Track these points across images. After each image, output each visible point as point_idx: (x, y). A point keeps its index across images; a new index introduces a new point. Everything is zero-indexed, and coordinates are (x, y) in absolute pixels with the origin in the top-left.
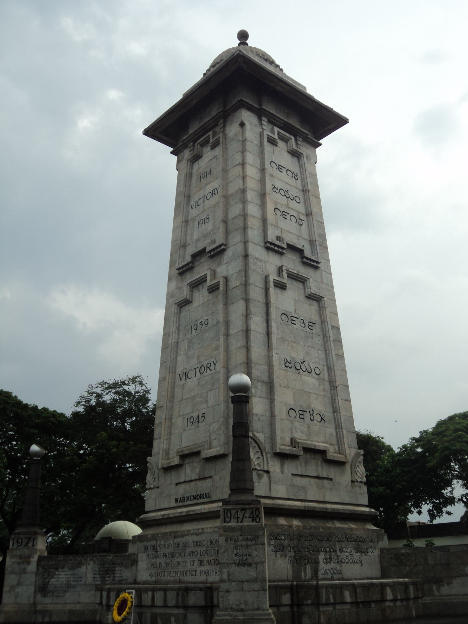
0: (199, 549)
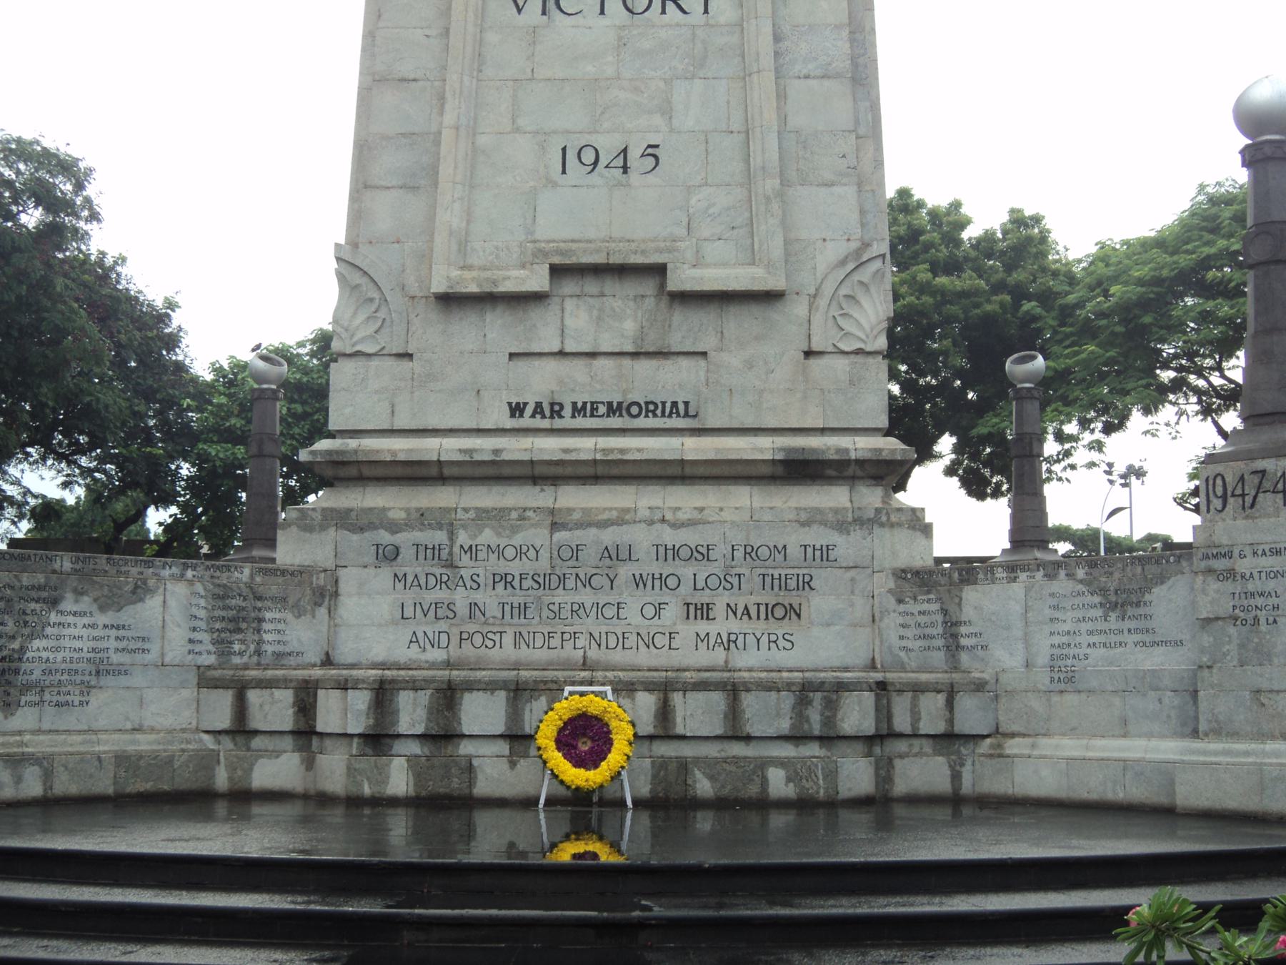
0: (687, 571)
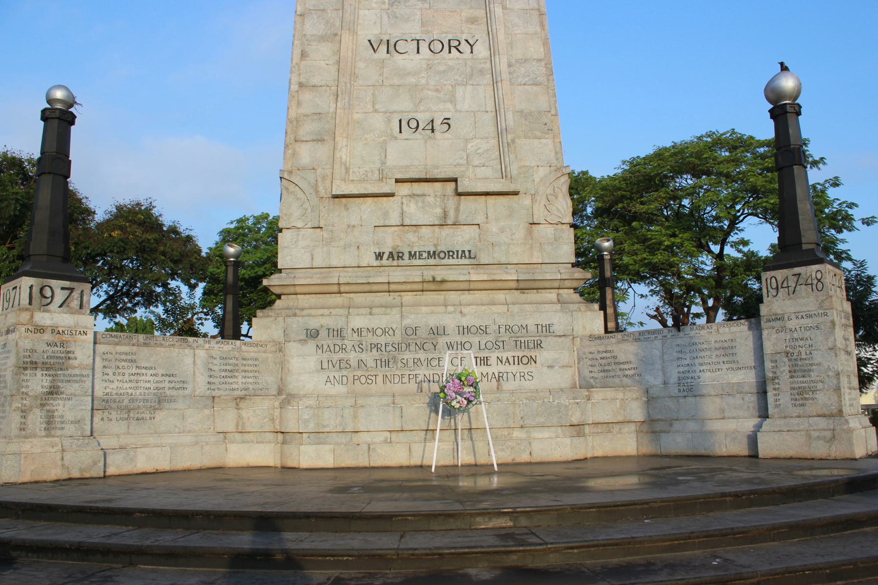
0: (475, 340)
